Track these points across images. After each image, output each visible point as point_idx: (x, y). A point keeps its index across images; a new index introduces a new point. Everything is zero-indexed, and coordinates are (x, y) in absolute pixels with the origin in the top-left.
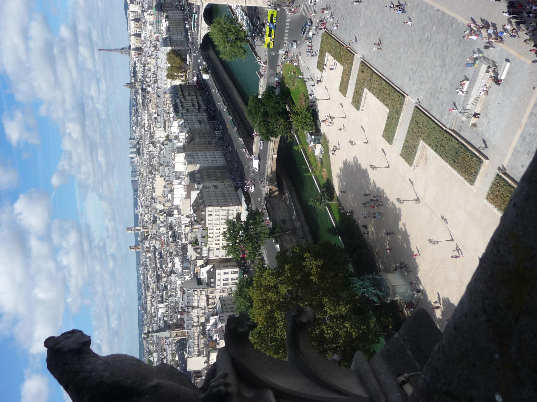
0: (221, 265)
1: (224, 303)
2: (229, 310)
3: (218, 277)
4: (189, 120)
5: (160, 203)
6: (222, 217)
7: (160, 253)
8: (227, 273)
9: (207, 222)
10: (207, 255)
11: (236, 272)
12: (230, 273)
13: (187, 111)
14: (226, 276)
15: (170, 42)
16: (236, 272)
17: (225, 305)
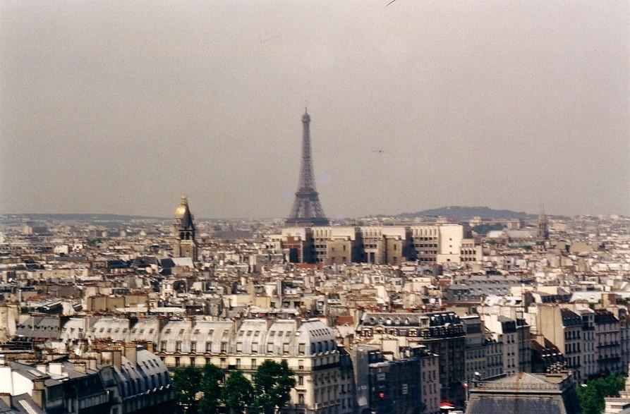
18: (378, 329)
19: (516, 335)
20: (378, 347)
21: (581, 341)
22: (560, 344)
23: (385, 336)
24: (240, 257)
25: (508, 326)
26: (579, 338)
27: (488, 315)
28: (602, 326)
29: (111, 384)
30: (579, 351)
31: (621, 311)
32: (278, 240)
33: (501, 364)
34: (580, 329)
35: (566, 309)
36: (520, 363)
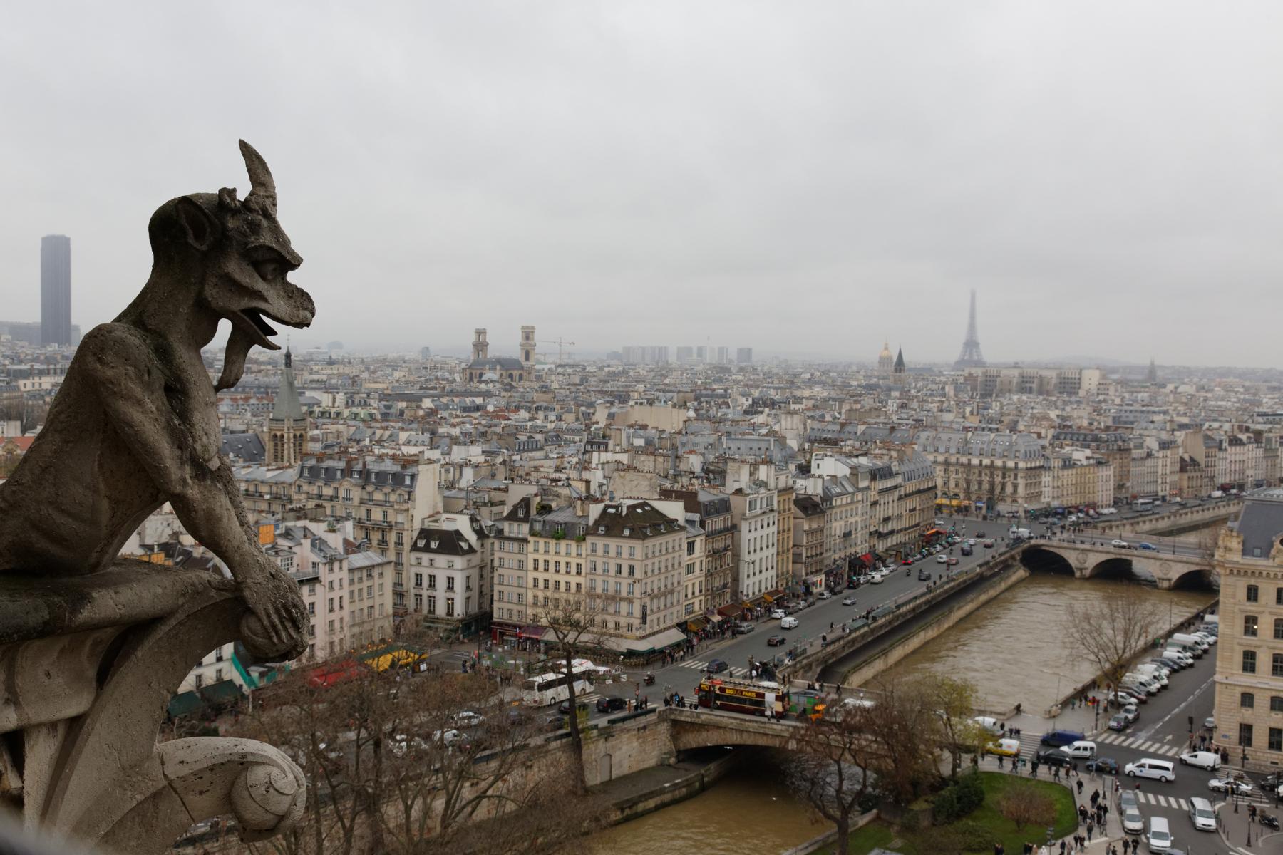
0: (475, 573)
1: (376, 573)
2: (356, 587)
3: (442, 560)
5: (611, 416)
6: (612, 581)
7: (478, 408)
8: (450, 587)
9: (600, 542)
10: (506, 534)
11: (450, 612)
12: (451, 595)
13: (874, 504)
14: (441, 583)
15: (1035, 468)
16: (450, 612)
17: (370, 576)
19: (1169, 453)
22: (1201, 459)
31: (1249, 438)
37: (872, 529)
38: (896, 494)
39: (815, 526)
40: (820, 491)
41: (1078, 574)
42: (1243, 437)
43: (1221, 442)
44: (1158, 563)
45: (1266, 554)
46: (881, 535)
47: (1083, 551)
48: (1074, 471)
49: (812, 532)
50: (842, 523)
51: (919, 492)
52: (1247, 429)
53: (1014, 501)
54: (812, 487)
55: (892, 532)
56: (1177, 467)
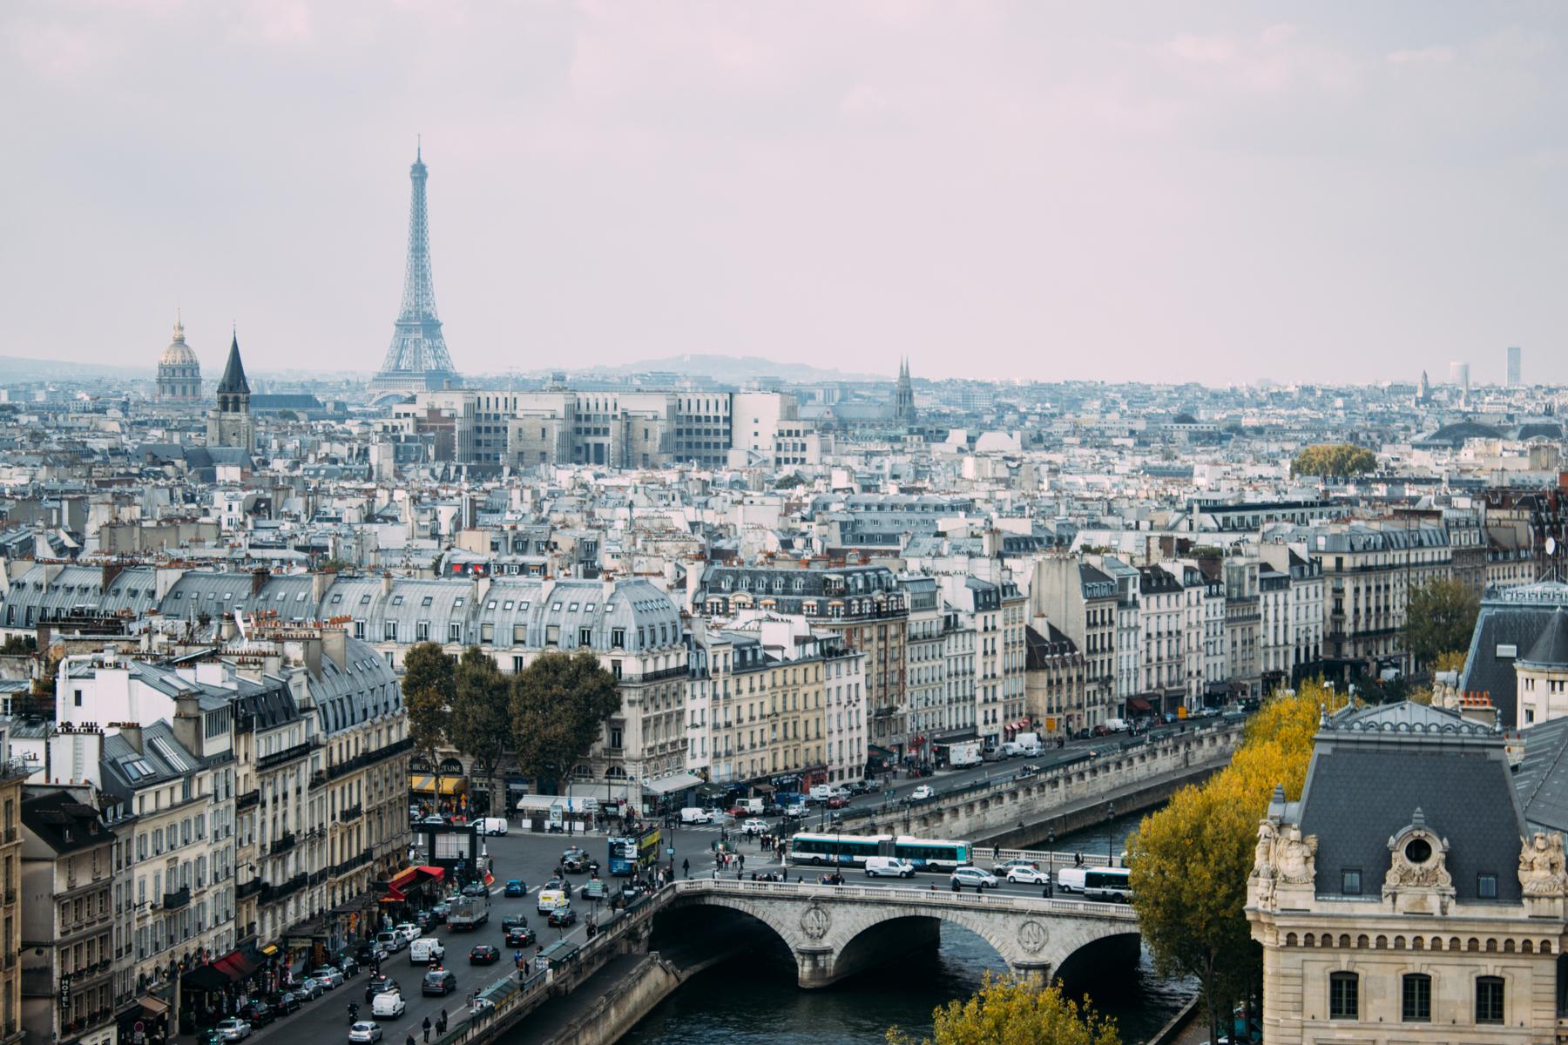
4: (191, 812)
13: (248, 802)
18: (740, 599)
20: (754, 635)
21: (1114, 630)
22: (1077, 632)
23: (763, 614)
24: (351, 449)
25: (988, 599)
26: (1111, 622)
27: (947, 574)
28: (1153, 599)
29: (309, 709)
30: (1111, 649)
31: (1187, 570)
32: (407, 415)
33: (972, 673)
34: (1114, 606)
35: (1088, 565)
36: (1007, 672)
37: (245, 877)
38: (306, 770)
39: (84, 880)
40: (91, 772)
41: (805, 969)
42: (1175, 567)
43: (1123, 581)
44: (1014, 922)
45: (1372, 886)
46: (266, 895)
47: (818, 901)
48: (768, 676)
49: (75, 900)
50: (161, 865)
51: (368, 759)
52: (1184, 547)
53: (615, 772)
54: (71, 764)
55: (298, 884)
56: (1020, 659)
